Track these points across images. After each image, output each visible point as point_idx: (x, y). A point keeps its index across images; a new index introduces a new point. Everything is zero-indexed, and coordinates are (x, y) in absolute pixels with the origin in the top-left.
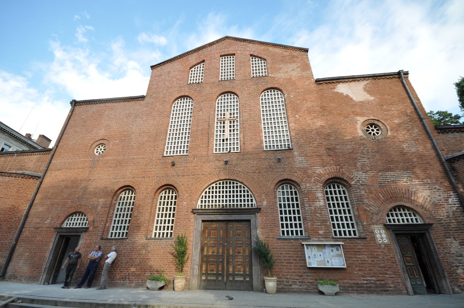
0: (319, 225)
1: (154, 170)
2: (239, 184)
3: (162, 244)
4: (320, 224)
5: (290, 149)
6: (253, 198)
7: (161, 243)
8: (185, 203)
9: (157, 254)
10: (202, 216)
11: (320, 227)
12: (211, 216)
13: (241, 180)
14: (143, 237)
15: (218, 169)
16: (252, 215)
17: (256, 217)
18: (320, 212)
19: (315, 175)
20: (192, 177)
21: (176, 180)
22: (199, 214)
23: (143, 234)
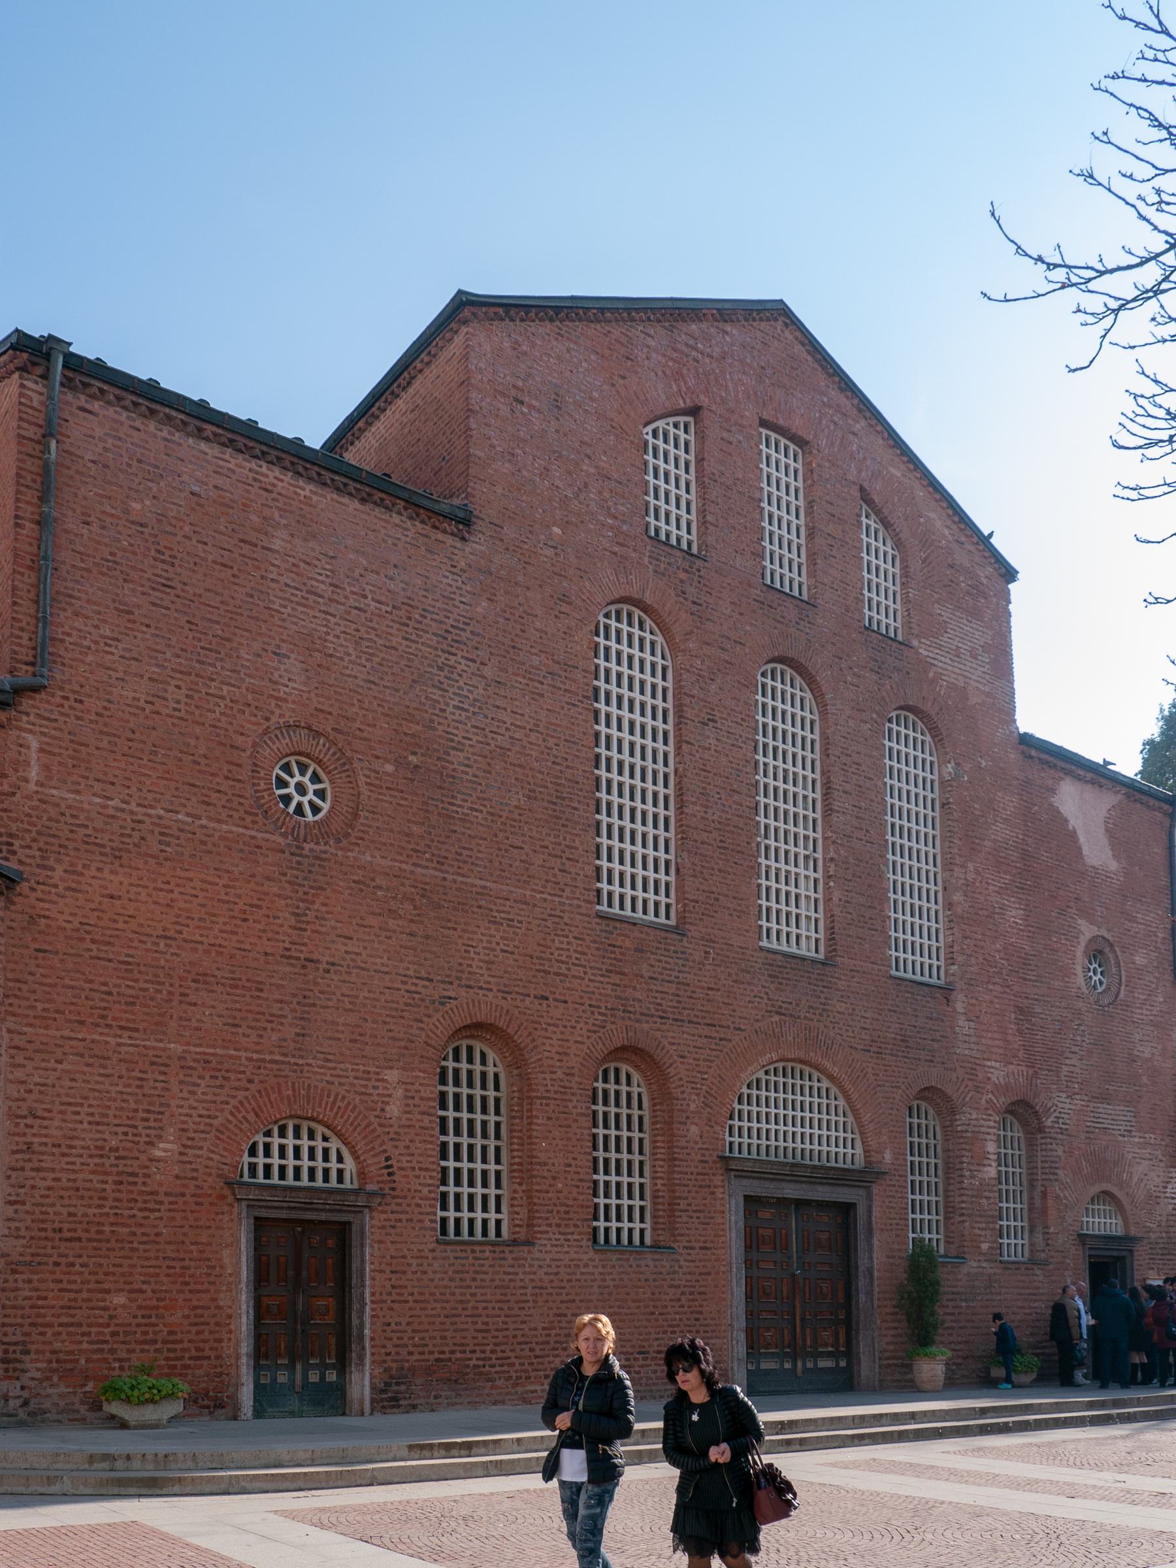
0: (982, 1229)
1: (576, 971)
2: (825, 1084)
3: (643, 1269)
4: (984, 1225)
5: (946, 991)
6: (857, 1136)
7: (642, 1263)
8: (694, 1129)
9: (634, 1301)
10: (745, 1182)
11: (983, 1233)
12: (767, 1184)
13: (835, 1071)
14: (584, 1243)
15: (776, 1018)
16: (862, 1192)
17: (870, 1197)
18: (987, 1194)
19: (989, 1087)
20: (706, 1031)
21: (658, 1034)
22: (742, 1174)
23: (582, 1230)
